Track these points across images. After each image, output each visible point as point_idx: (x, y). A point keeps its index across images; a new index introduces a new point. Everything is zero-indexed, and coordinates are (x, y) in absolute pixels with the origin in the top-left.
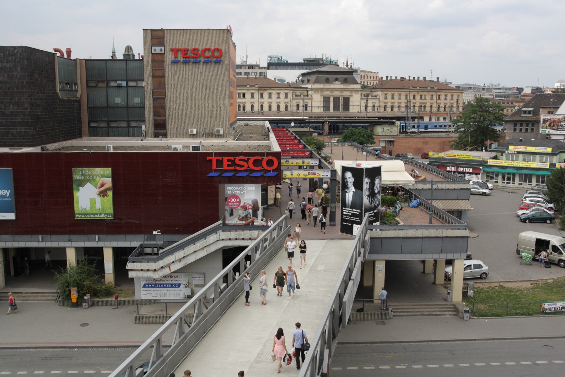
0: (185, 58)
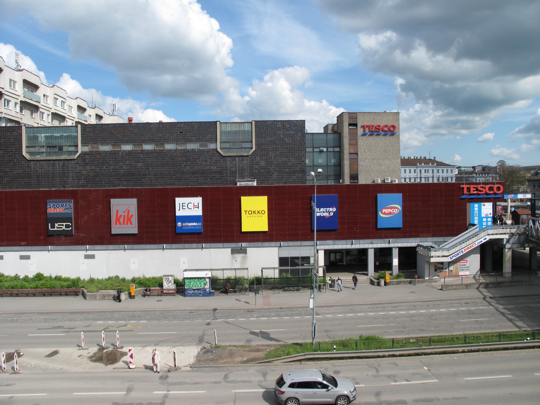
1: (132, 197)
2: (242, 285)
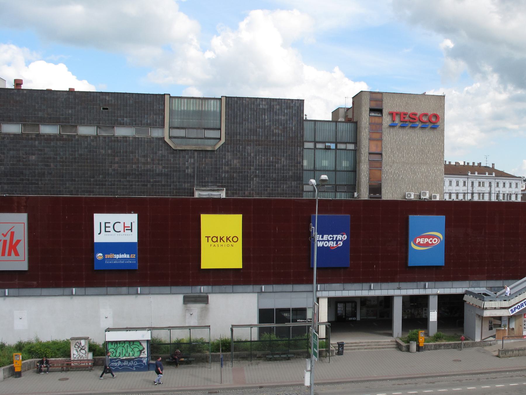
0: (403, 122)
1: (19, 211)
2: (199, 351)
